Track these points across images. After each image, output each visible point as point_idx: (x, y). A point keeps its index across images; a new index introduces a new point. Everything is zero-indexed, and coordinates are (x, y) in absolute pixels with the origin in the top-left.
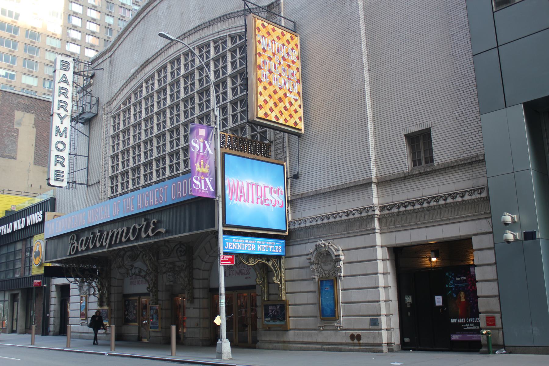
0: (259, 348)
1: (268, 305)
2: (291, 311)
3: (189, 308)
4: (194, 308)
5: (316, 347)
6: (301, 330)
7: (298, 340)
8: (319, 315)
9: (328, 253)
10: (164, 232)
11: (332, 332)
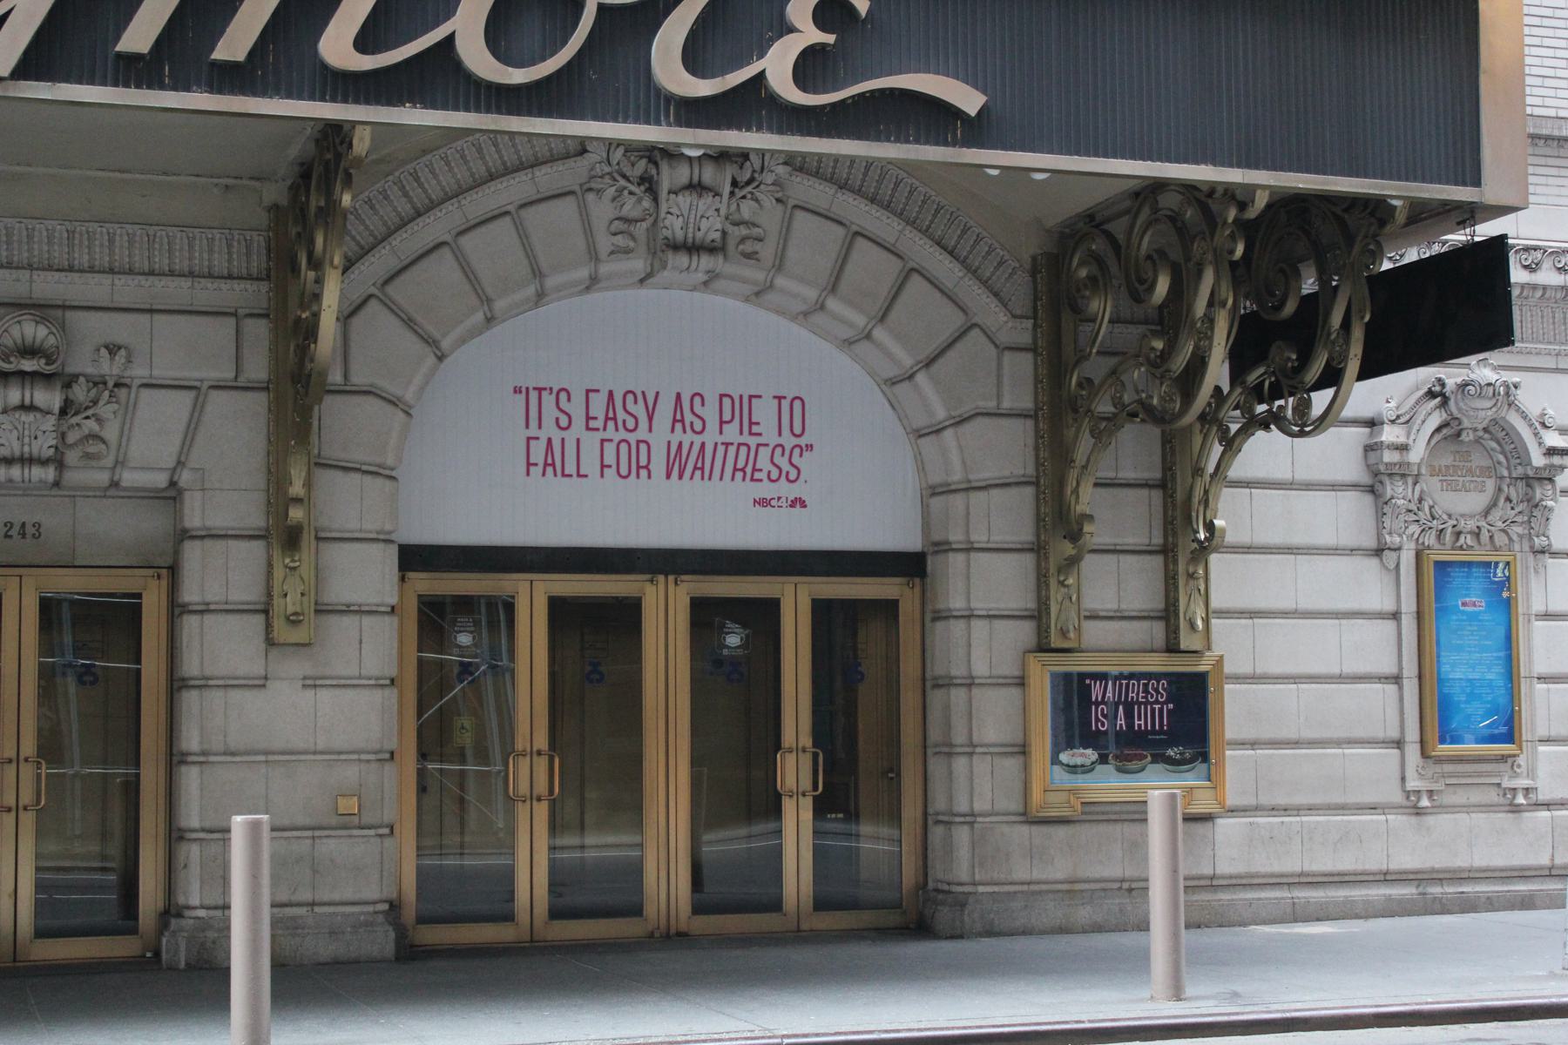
0: (990, 932)
1: (1082, 676)
2: (1235, 711)
3: (261, 683)
4: (312, 683)
5: (1389, 899)
6: (1286, 810)
7: (1277, 868)
8: (1412, 734)
9: (1500, 435)
10: (973, 112)
11: (1479, 818)
